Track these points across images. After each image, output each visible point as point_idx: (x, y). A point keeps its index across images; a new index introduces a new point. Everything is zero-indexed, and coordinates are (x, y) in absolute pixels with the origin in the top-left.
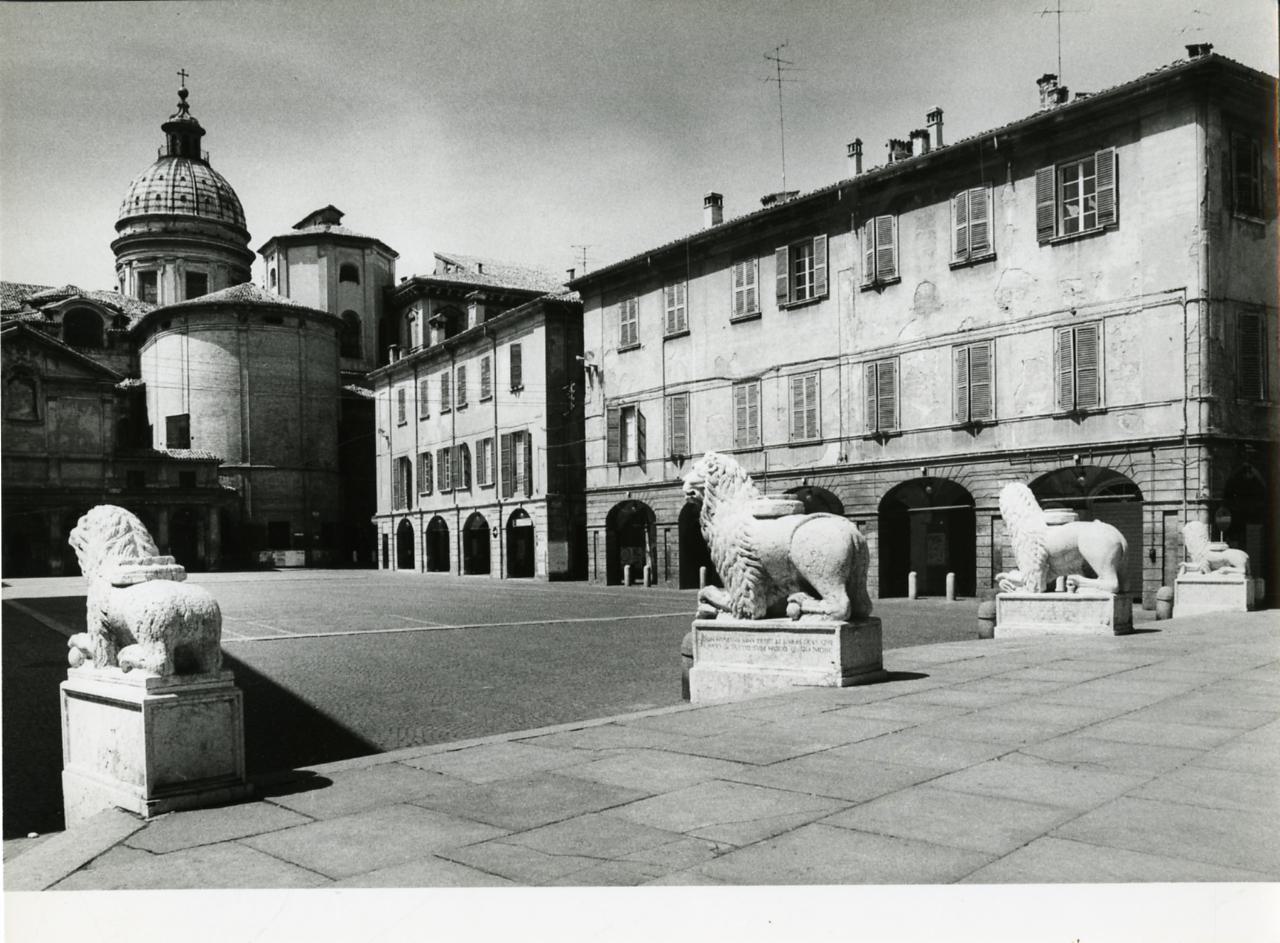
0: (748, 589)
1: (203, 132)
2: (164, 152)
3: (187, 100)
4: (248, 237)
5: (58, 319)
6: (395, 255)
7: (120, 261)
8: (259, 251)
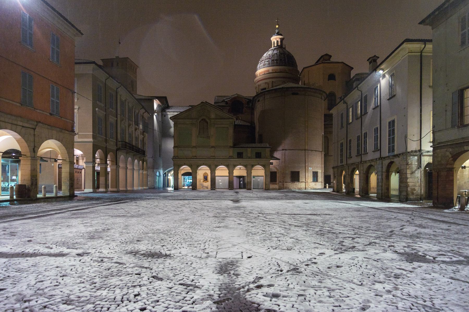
6: (352, 68)
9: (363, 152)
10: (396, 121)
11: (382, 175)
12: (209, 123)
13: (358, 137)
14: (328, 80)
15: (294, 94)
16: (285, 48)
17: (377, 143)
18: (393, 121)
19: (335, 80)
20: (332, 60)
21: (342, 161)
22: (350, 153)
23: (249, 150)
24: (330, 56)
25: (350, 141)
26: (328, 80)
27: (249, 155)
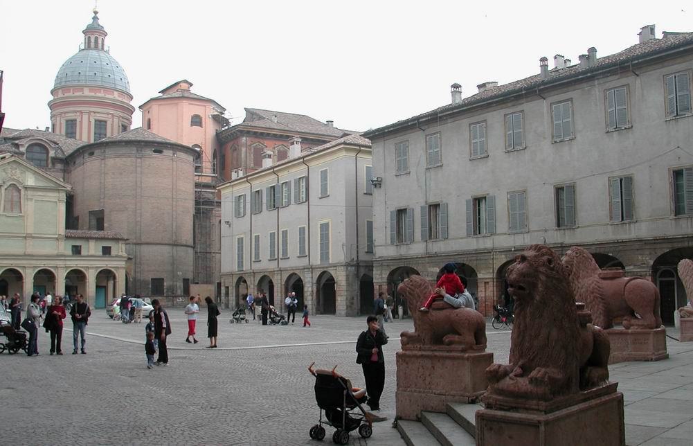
0: (600, 313)
1: (106, 34)
2: (83, 47)
3: (97, 15)
4: (131, 98)
5: (23, 149)
7: (54, 113)
8: (140, 107)
9: (281, 256)
10: (330, 224)
11: (312, 287)
12: (22, 192)
13: (272, 235)
14: (192, 125)
15: (155, 151)
16: (107, 52)
17: (304, 246)
18: (327, 225)
19: (201, 126)
20: (193, 90)
21: (240, 264)
22: (257, 255)
23: (92, 243)
24: (191, 85)
25: (257, 238)
26: (192, 125)
27: (92, 252)
